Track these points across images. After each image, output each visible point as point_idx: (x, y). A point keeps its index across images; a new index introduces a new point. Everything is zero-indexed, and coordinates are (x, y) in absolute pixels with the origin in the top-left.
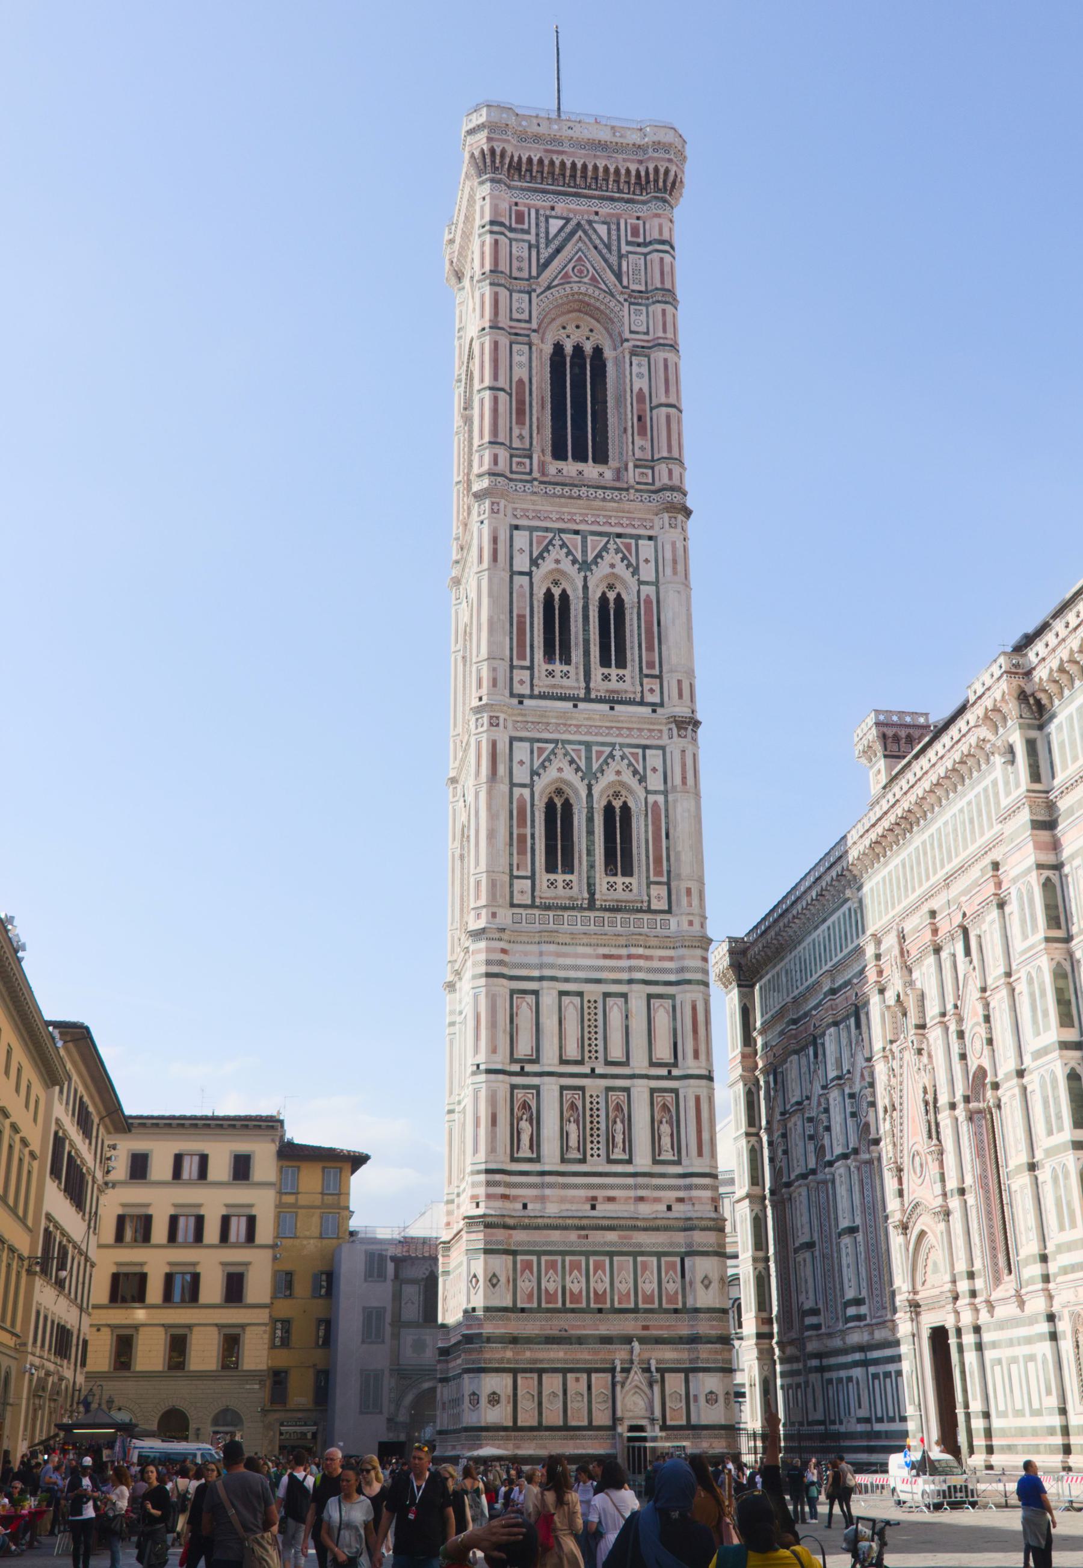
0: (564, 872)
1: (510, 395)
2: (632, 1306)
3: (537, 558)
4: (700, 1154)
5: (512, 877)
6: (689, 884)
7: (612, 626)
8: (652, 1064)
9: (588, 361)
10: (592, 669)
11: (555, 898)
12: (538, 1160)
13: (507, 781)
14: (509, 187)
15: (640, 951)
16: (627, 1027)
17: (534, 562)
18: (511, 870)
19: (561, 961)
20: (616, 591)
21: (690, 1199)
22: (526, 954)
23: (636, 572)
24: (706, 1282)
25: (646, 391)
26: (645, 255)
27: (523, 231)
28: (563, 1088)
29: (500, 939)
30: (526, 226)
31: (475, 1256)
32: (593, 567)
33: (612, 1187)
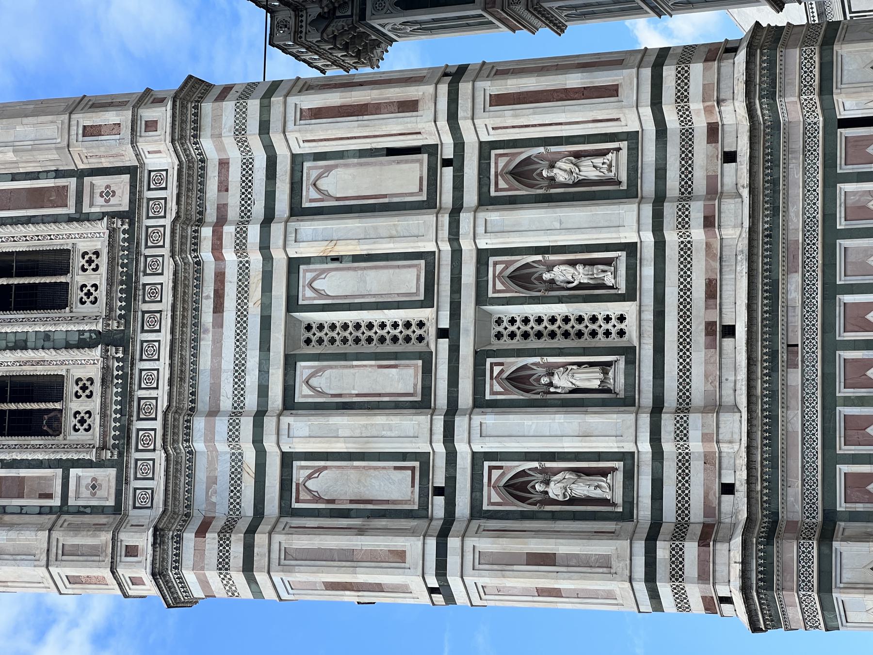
0: (59, 398)
4: (611, 91)
5: (64, 509)
6: (76, 131)
8: (430, 204)
11: (104, 415)
12: (628, 458)
15: (207, 232)
16: (356, 258)
18: (51, 510)
19: (226, 403)
21: (708, 110)
22: (212, 481)
28: (480, 403)
29: (179, 539)
31: (839, 609)
33: (685, 289)
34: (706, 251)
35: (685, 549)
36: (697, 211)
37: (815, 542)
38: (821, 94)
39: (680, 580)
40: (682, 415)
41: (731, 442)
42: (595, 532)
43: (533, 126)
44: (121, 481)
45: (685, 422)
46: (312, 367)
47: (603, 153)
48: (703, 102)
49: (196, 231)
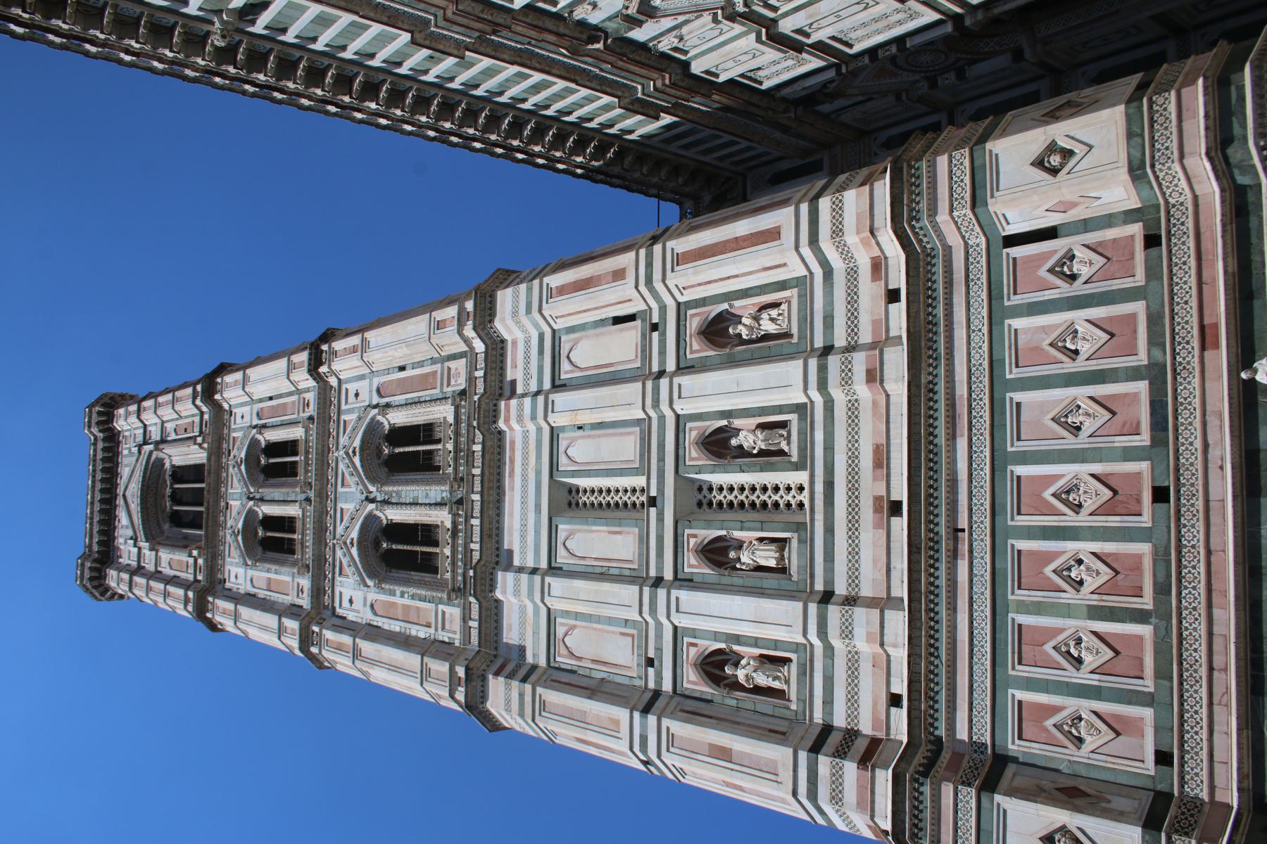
2: (1142, 387)
4: (772, 235)
21: (864, 242)
24: (1055, 160)
33: (853, 457)
34: (873, 411)
35: (845, 770)
36: (860, 361)
37: (974, 790)
38: (973, 207)
39: (840, 804)
40: (847, 608)
41: (895, 646)
42: (771, 731)
43: (716, 281)
45: (851, 616)
46: (567, 530)
47: (775, 305)
48: (858, 233)
49: (495, 405)
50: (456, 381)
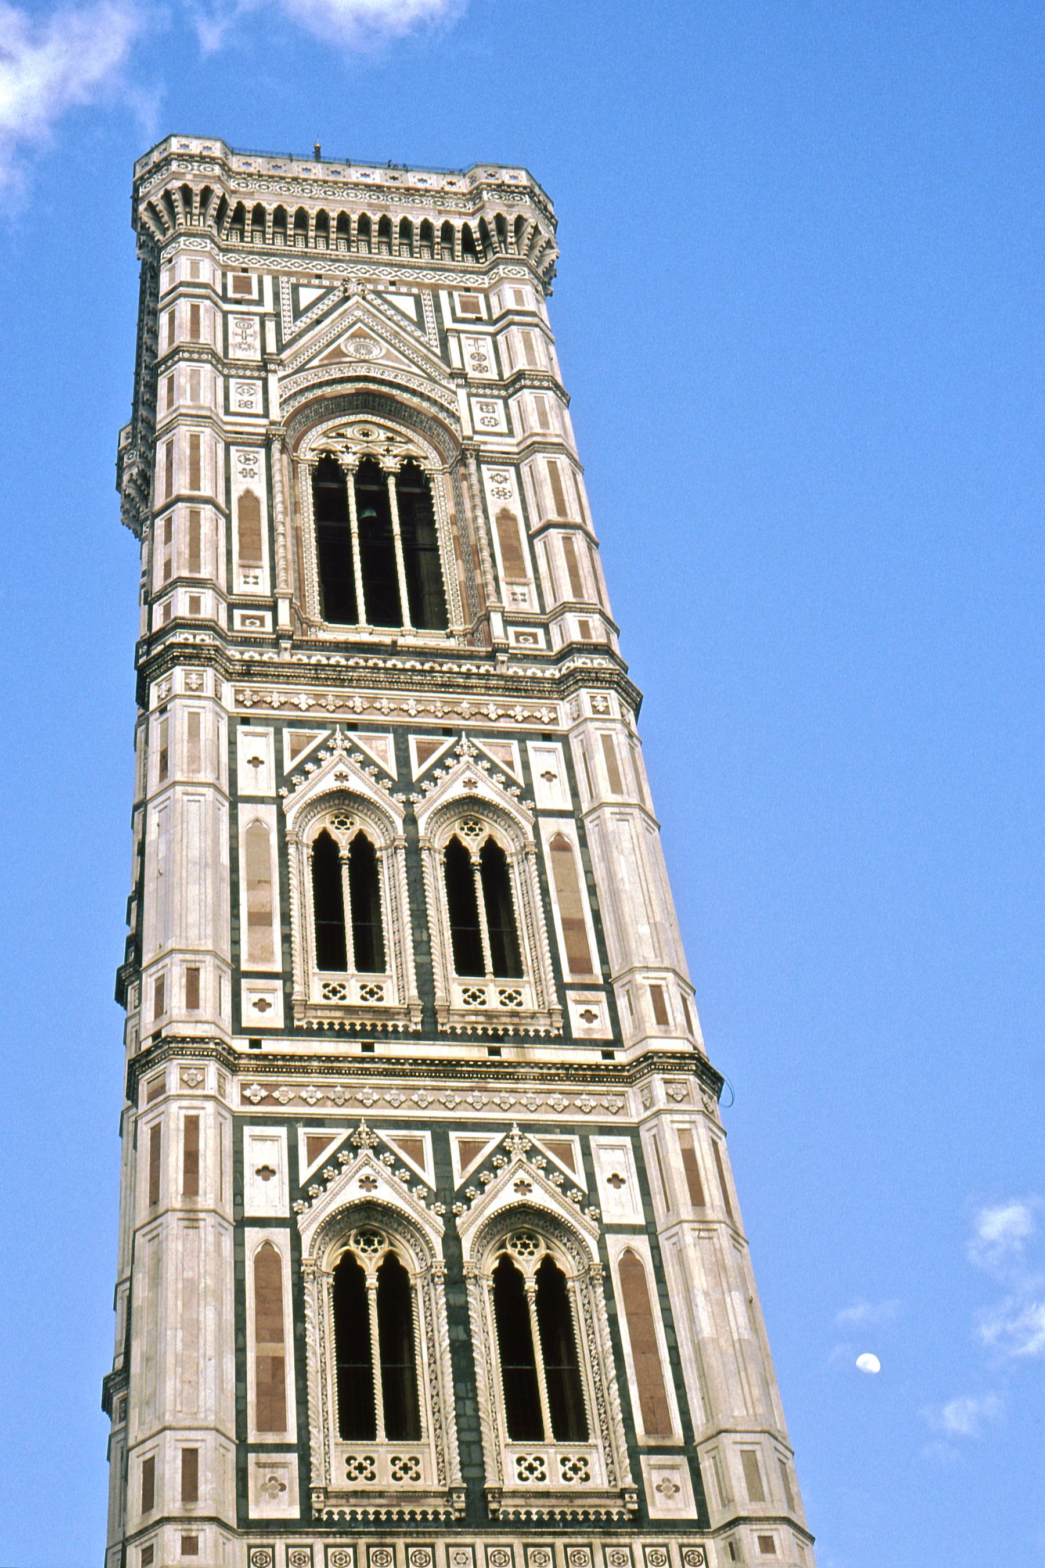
1: (228, 518)
3: (292, 773)
5: (243, 1447)
7: (481, 902)
9: (391, 481)
10: (438, 977)
13: (229, 1211)
14: (218, 247)
17: (283, 780)
20: (483, 837)
23: (527, 793)
25: (516, 510)
26: (494, 335)
27: (250, 302)
30: (255, 296)
32: (425, 785)
44: (283, 1527)
50: (658, 1488)
